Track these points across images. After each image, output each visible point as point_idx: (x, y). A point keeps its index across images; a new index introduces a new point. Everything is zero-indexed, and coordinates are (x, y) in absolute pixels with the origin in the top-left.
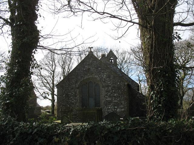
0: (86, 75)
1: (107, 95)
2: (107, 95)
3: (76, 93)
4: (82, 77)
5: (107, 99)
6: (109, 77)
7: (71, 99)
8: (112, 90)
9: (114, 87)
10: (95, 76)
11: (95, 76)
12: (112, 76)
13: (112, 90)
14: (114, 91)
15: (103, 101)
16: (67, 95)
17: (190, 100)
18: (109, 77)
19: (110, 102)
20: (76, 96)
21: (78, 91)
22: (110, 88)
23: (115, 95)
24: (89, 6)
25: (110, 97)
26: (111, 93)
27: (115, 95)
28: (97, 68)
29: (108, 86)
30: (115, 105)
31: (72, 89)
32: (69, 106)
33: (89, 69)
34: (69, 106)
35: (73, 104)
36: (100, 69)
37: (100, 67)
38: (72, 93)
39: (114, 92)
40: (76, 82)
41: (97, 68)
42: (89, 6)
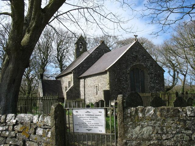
0: (135, 61)
1: (151, 81)
2: (151, 81)
3: (126, 78)
4: (131, 63)
5: (151, 85)
6: (152, 66)
7: (123, 84)
8: (155, 77)
9: (156, 75)
10: (142, 64)
11: (142, 64)
12: (154, 65)
13: (155, 77)
14: (155, 78)
15: (149, 87)
16: (119, 80)
17: (134, 136)
18: (152, 66)
19: (154, 87)
20: (127, 81)
21: (128, 76)
22: (153, 75)
23: (157, 81)
24: (71, 10)
25: (153, 83)
26: (154, 80)
27: (157, 81)
28: (143, 56)
29: (152, 73)
30: (157, 91)
31: (123, 73)
32: (121, 91)
33: (137, 56)
34: (121, 91)
35: (125, 89)
36: (145, 57)
37: (145, 55)
38: (124, 78)
39: (156, 79)
40: (127, 67)
41: (143, 56)
42: (71, 10)
